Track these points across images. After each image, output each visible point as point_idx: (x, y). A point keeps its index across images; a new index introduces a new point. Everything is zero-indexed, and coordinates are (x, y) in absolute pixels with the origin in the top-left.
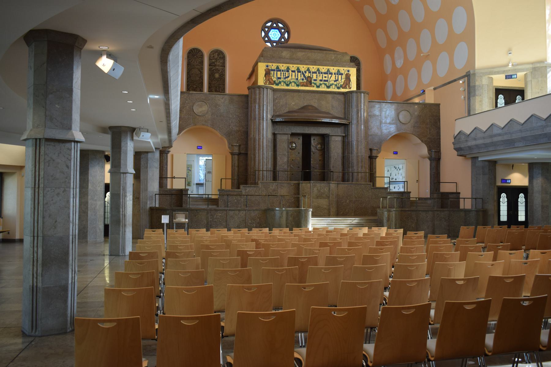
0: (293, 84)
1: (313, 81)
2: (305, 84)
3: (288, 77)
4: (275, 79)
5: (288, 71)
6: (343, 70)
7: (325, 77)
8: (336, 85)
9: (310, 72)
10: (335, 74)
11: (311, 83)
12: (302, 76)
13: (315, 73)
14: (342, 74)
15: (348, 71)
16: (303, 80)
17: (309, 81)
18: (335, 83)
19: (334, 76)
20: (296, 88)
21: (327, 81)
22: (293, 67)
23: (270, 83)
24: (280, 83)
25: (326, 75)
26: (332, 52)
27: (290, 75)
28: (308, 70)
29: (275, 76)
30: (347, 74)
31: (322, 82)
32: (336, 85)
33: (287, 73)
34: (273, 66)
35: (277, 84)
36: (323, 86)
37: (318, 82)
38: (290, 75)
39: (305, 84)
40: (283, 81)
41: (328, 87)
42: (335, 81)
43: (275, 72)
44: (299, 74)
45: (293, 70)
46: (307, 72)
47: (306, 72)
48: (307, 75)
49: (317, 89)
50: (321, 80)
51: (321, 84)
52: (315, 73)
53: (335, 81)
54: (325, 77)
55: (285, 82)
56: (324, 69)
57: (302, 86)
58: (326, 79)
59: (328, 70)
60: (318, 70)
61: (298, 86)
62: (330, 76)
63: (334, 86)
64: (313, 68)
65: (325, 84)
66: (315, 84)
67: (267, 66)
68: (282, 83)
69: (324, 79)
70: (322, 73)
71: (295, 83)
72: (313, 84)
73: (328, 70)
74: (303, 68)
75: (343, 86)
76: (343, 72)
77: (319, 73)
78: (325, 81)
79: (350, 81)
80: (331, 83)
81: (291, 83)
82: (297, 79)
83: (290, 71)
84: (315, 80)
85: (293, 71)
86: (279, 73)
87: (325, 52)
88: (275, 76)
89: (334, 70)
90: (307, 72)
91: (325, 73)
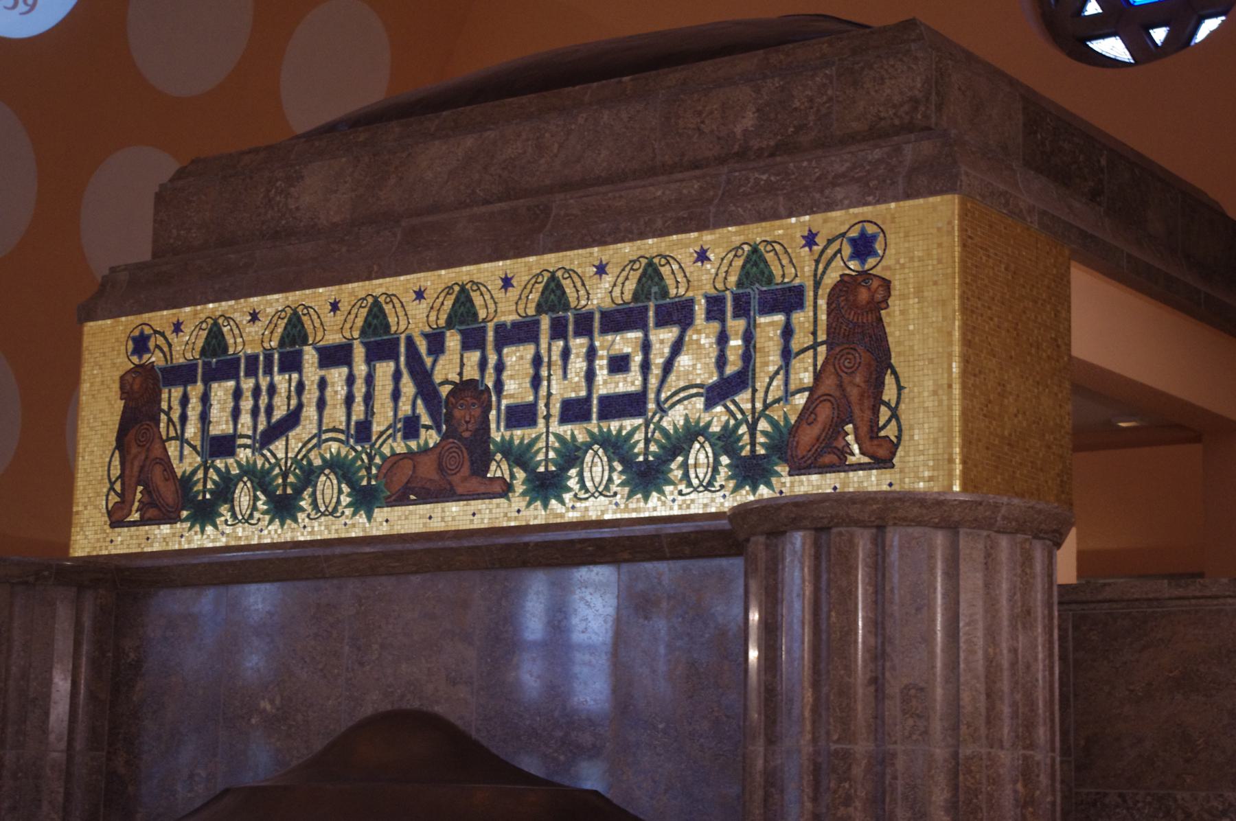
0: (327, 486)
1: (497, 434)
2: (427, 469)
3: (293, 419)
4: (185, 462)
5: (292, 363)
6: (797, 244)
7: (619, 364)
8: (726, 442)
9: (473, 340)
10: (715, 308)
11: (479, 450)
12: (408, 387)
13: (523, 332)
14: (787, 300)
15: (863, 246)
16: (411, 427)
17: (463, 442)
18: (718, 418)
19: (703, 336)
20: (358, 526)
21: (631, 404)
22: (333, 309)
23: (159, 512)
24: (225, 491)
25: (626, 342)
26: (746, 63)
27: (311, 395)
28: (463, 313)
29: (191, 430)
30: (845, 286)
31: (578, 432)
32: (726, 442)
33: (280, 380)
34: (181, 330)
35: (204, 514)
36: (596, 466)
37: (546, 436)
38: (311, 395)
39: (427, 469)
40: (248, 471)
41: (646, 477)
42: (717, 393)
43: (195, 391)
44: (385, 369)
45: (333, 338)
46: (453, 341)
47: (436, 343)
48: (451, 366)
49: (537, 515)
50: (574, 411)
51: (571, 455)
52: (523, 332)
53: (717, 393)
54: (619, 364)
55: (261, 480)
56: (600, 275)
57: (401, 499)
58: (628, 383)
59: (651, 274)
60: (553, 294)
61: (365, 500)
62: (663, 338)
63: (700, 454)
64: (504, 285)
65: (616, 448)
66: (520, 457)
67: (140, 344)
68: (243, 497)
69: (607, 383)
70: (584, 326)
71: (339, 467)
72: (498, 469)
73: (651, 274)
74: (415, 299)
75: (809, 435)
76: (805, 277)
77: (559, 331)
78: (617, 406)
79: (880, 360)
80: (675, 418)
81: (309, 476)
82: (363, 431)
83: (310, 356)
84: (522, 415)
85: (334, 356)
86: (221, 391)
87: (673, 77)
88: (191, 430)
89: (700, 260)
90: (453, 341)
91: (617, 320)
